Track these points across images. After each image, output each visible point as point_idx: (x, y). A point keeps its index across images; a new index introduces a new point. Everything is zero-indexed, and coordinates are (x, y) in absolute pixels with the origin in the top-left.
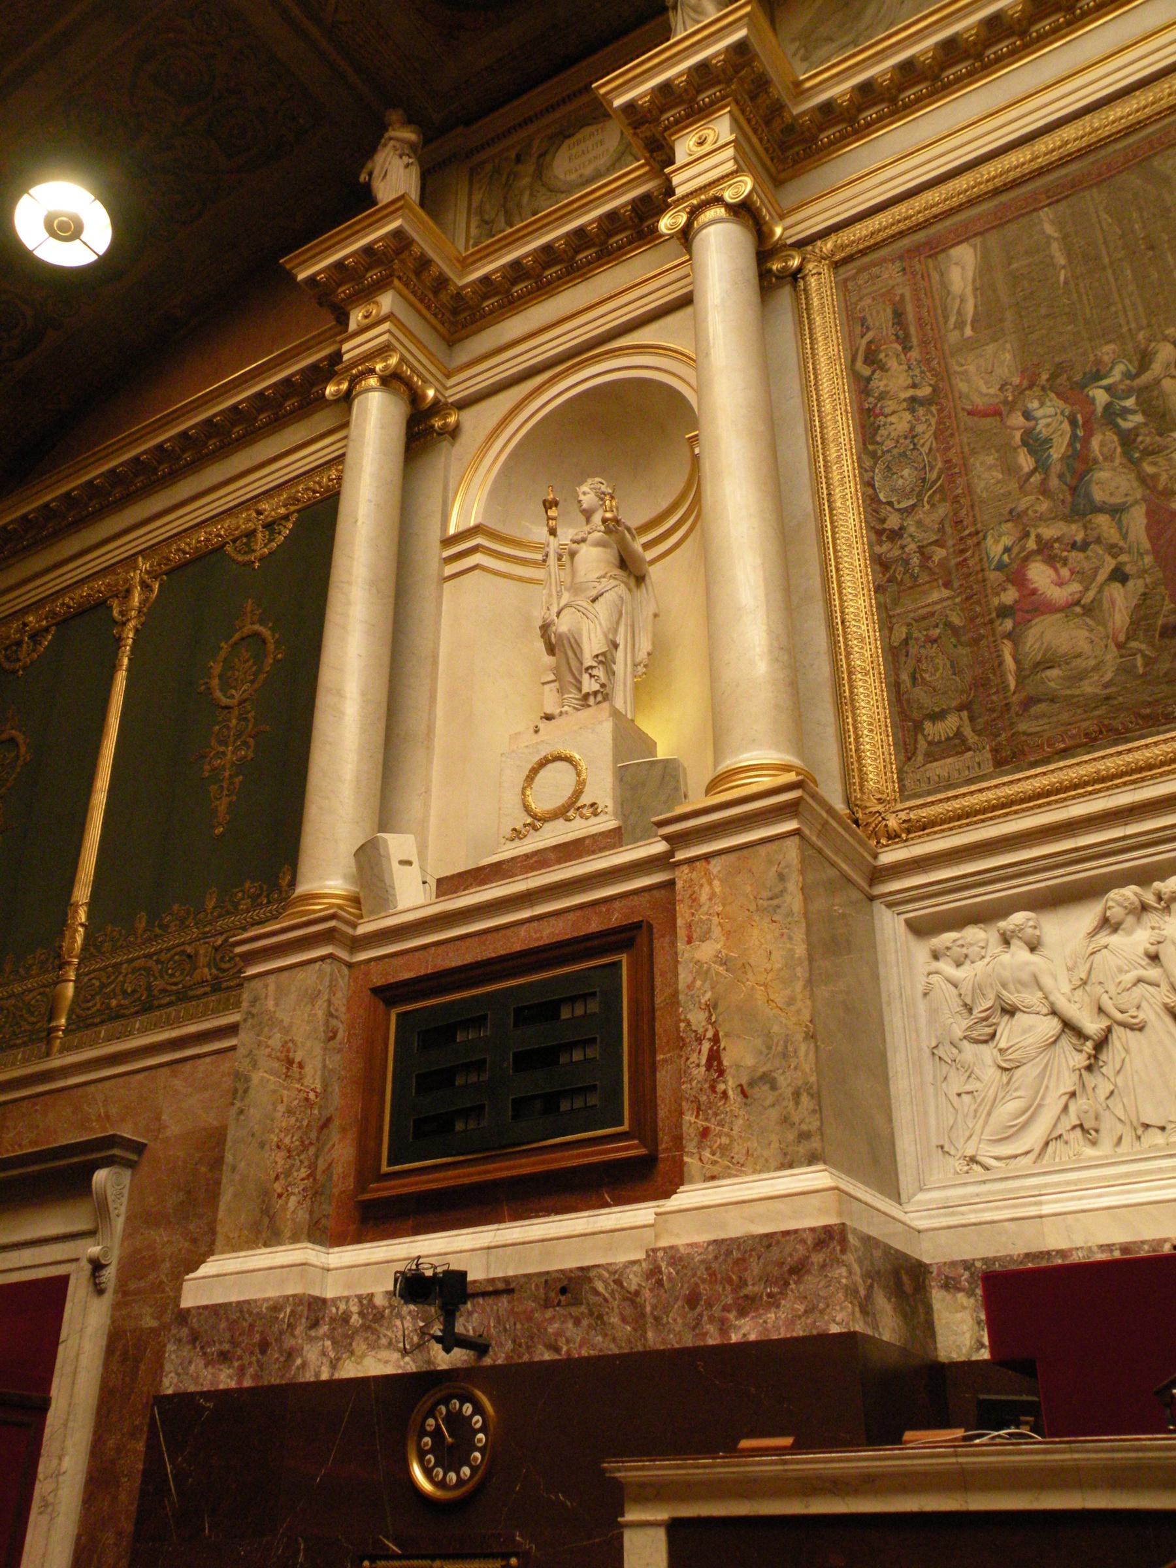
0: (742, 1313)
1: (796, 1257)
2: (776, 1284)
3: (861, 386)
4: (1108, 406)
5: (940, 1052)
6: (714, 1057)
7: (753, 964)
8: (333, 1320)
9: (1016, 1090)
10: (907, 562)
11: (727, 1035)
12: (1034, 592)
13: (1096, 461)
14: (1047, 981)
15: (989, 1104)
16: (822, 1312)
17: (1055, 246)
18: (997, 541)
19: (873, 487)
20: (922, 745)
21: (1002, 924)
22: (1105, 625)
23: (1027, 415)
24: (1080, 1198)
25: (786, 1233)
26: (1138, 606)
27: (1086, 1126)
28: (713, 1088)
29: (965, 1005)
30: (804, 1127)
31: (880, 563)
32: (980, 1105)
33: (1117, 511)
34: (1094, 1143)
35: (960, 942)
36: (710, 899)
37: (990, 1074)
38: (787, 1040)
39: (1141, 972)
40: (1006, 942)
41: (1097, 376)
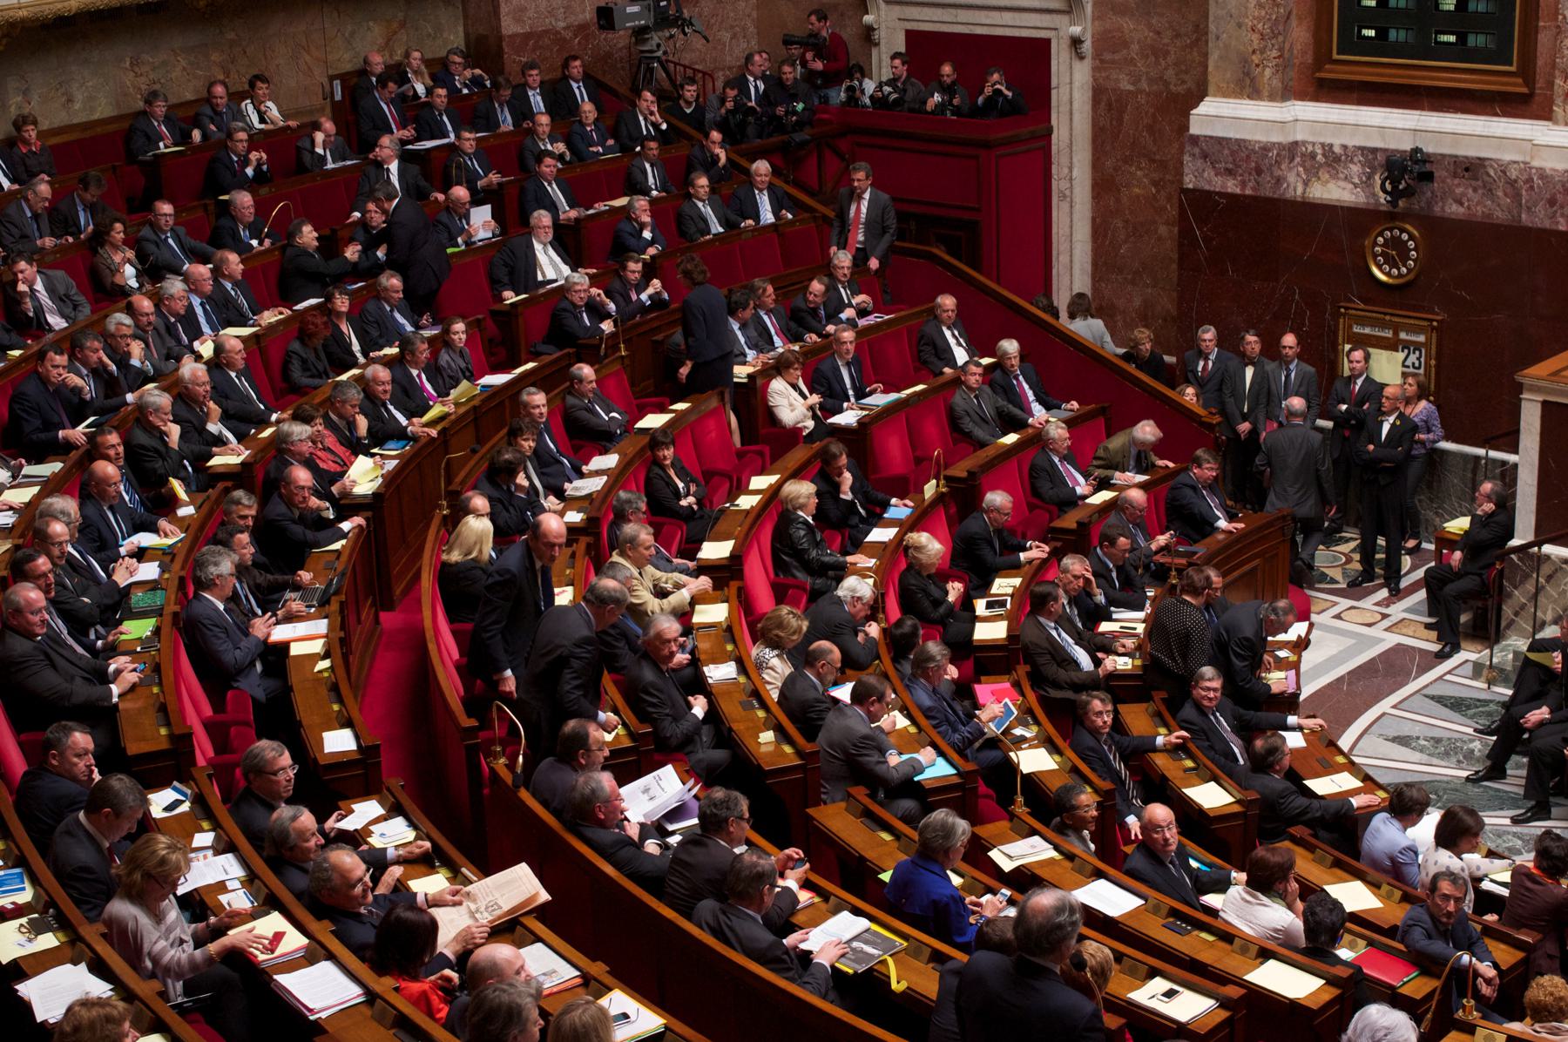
8: (1303, 155)
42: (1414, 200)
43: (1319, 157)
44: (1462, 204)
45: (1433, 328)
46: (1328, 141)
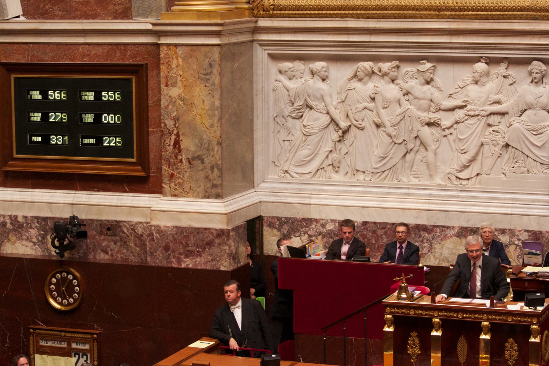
0: (187, 256)
1: (209, 239)
2: (200, 247)
5: (278, 120)
6: (177, 143)
9: (308, 145)
11: (183, 134)
14: (327, 99)
15: (296, 148)
16: (218, 261)
24: (327, 199)
25: (206, 229)
27: (334, 165)
28: (176, 157)
30: (215, 182)
32: (292, 147)
34: (337, 172)
35: (291, 70)
36: (177, 67)
37: (298, 134)
38: (209, 143)
39: (366, 104)
42: (75, 251)
43: (9, 225)
44: (107, 253)
45: (94, 339)
46: (14, 214)
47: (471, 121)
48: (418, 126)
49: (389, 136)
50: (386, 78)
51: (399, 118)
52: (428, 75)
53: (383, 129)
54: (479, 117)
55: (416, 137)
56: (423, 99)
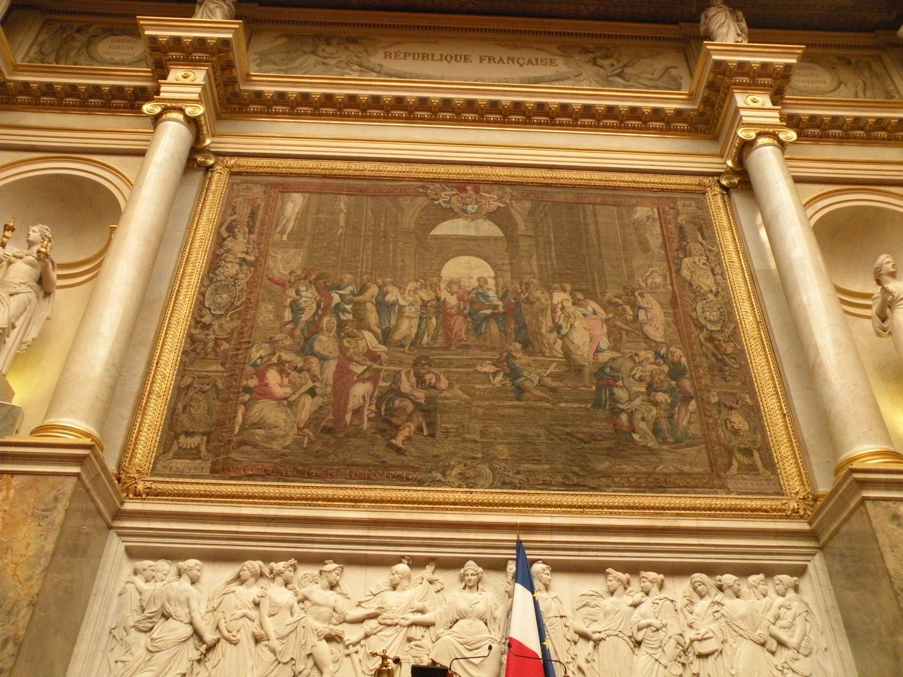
3: (220, 241)
4: (338, 305)
5: (115, 632)
7: (14, 548)
9: (152, 665)
10: (206, 344)
12: (266, 385)
13: (322, 330)
14: (194, 604)
17: (342, 215)
18: (257, 351)
19: (204, 296)
20: (175, 448)
21: (181, 564)
22: (295, 415)
23: (298, 292)
26: (316, 412)
29: (142, 606)
31: (191, 338)
33: (323, 359)
39: (246, 611)
40: (180, 575)
41: (338, 288)
47: (389, 631)
48: (314, 640)
49: (273, 651)
50: (279, 580)
51: (289, 628)
52: (333, 577)
53: (266, 642)
54: (398, 627)
55: (309, 655)
56: (325, 605)
